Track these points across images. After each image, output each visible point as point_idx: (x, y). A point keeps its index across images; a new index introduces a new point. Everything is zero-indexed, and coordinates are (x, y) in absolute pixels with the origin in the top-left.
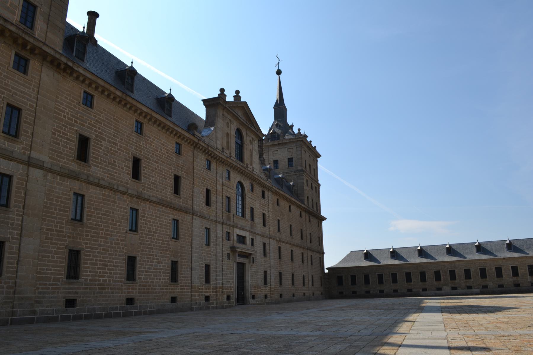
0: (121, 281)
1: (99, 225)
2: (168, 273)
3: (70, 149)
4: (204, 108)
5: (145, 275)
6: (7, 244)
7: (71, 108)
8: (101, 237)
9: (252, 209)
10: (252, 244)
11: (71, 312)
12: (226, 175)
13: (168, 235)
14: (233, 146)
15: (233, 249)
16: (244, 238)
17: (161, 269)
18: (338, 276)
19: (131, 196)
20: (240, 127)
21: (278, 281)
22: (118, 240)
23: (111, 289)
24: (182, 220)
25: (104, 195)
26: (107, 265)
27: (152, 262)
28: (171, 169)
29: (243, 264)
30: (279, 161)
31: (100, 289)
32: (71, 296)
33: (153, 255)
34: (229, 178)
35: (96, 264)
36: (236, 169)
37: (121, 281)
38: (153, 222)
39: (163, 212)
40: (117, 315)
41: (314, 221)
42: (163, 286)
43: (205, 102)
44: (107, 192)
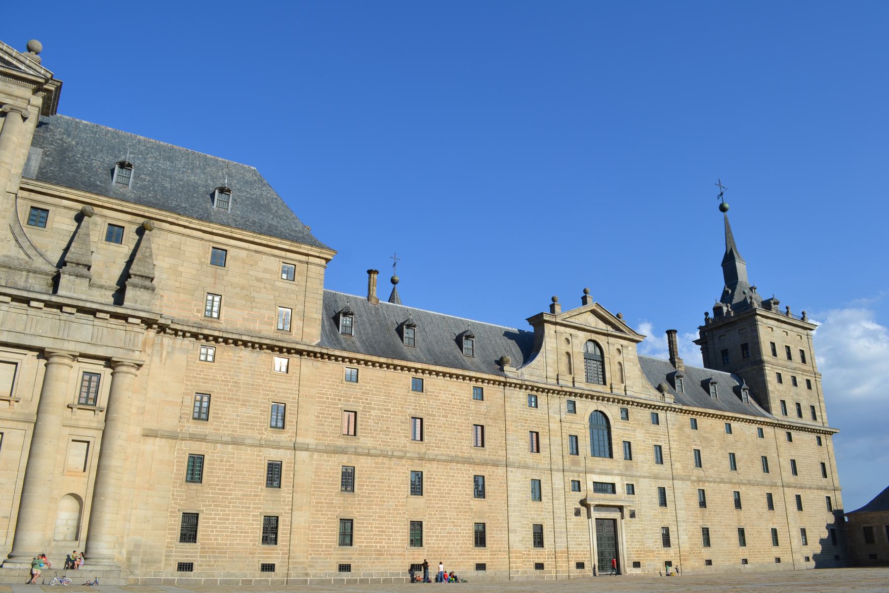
0: (403, 547)
3: (336, 426)
9: (628, 445)
11: (345, 575)
12: (564, 406)
16: (613, 485)
19: (411, 459)
22: (396, 505)
25: (376, 463)
28: (468, 419)
29: (615, 521)
32: (345, 562)
37: (403, 547)
39: (457, 469)
43: (531, 320)
44: (380, 460)
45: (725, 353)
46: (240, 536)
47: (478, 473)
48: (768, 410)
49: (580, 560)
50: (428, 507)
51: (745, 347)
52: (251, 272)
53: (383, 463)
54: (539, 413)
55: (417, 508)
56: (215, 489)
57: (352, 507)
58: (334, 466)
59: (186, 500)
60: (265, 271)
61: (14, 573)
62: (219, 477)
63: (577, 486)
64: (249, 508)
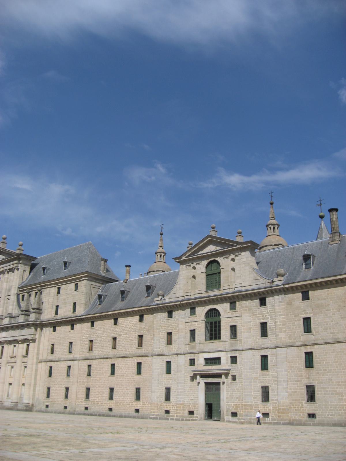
1: (97, 376)
2: (133, 395)
5: (119, 397)
7: (87, 332)
8: (98, 381)
9: (233, 329)
11: (86, 412)
13: (133, 373)
16: (219, 359)
17: (129, 393)
22: (105, 381)
24: (144, 362)
25: (99, 362)
26: (100, 393)
27: (123, 389)
28: (136, 333)
31: (97, 403)
32: (87, 406)
33: (124, 386)
38: (124, 368)
40: (103, 415)
42: (129, 402)
44: (100, 360)
47: (139, 361)
49: (191, 410)
50: (116, 381)
52: (66, 293)
53: (101, 362)
55: (112, 381)
57: (91, 383)
63: (192, 362)
64: (62, 385)
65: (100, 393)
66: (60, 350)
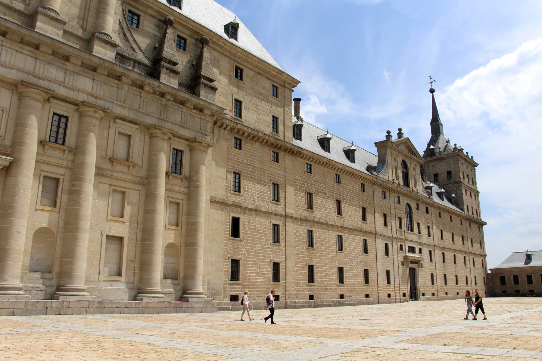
0: (336, 284)
4: (376, 149)
6: (281, 264)
9: (419, 224)
10: (420, 252)
12: (396, 200)
14: (400, 175)
15: (406, 257)
18: (501, 277)
20: (405, 159)
21: (443, 281)
23: (331, 289)
26: (327, 274)
28: (359, 203)
30: (439, 175)
32: (311, 294)
34: (399, 202)
35: (322, 273)
36: (404, 195)
41: (475, 226)
43: (376, 144)
45: (436, 175)
46: (261, 276)
48: (462, 210)
51: (449, 173)
52: (256, 88)
54: (386, 202)
56: (247, 242)
58: (303, 230)
59: (232, 250)
60: (264, 88)
61: (151, 305)
62: (248, 234)
63: (402, 249)
64: (265, 256)
65: (327, 274)
66: (256, 190)
